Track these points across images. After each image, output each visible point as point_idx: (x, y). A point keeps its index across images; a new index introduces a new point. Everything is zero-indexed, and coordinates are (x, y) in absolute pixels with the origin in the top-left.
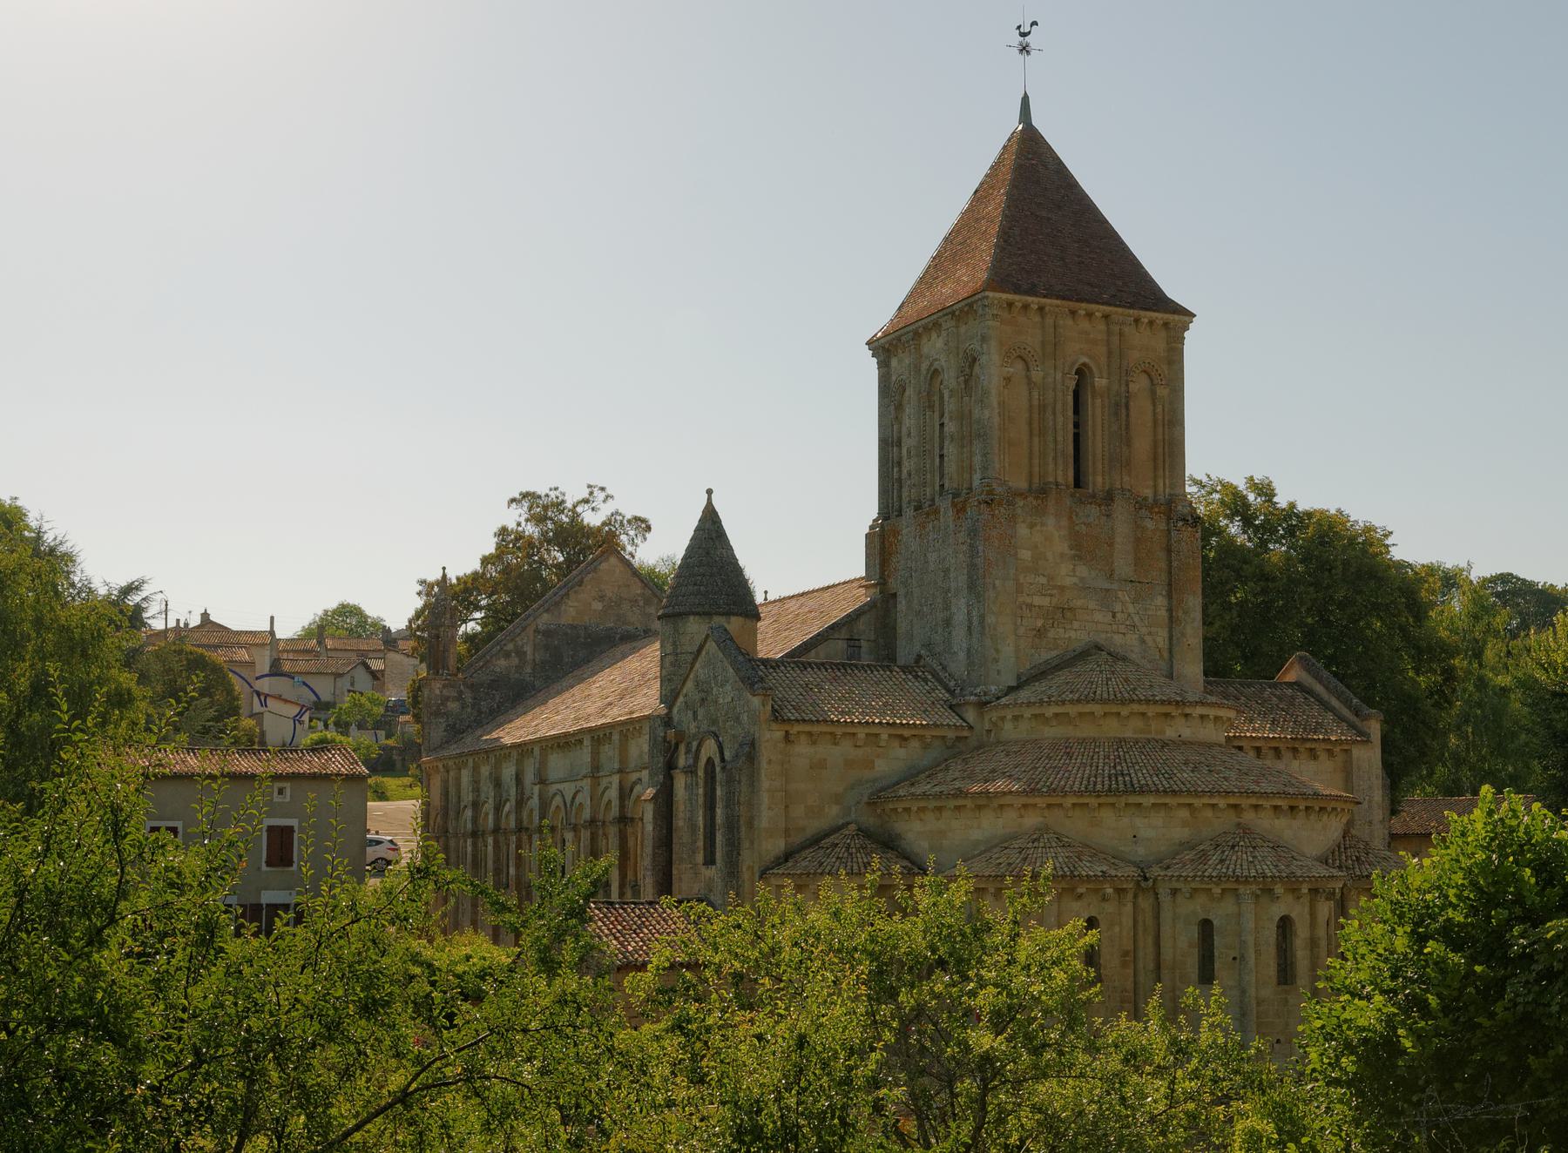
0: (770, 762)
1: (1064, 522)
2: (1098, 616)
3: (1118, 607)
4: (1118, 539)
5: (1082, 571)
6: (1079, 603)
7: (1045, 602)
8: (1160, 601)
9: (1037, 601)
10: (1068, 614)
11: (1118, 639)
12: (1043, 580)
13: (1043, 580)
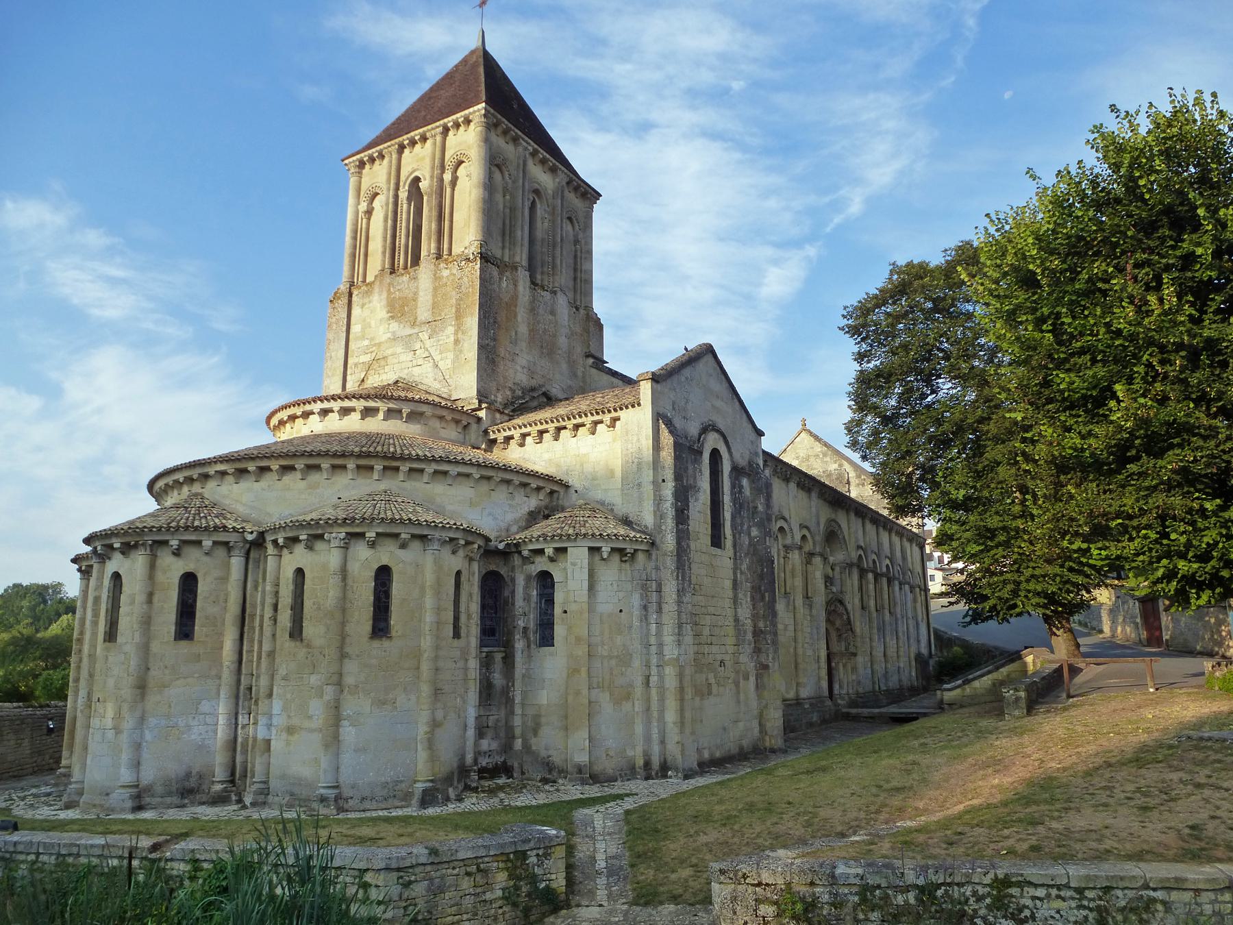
1: (385, 295)
2: (403, 358)
3: (417, 346)
4: (421, 294)
5: (394, 326)
6: (389, 352)
7: (366, 358)
10: (382, 363)
11: (416, 371)
13: (366, 343)
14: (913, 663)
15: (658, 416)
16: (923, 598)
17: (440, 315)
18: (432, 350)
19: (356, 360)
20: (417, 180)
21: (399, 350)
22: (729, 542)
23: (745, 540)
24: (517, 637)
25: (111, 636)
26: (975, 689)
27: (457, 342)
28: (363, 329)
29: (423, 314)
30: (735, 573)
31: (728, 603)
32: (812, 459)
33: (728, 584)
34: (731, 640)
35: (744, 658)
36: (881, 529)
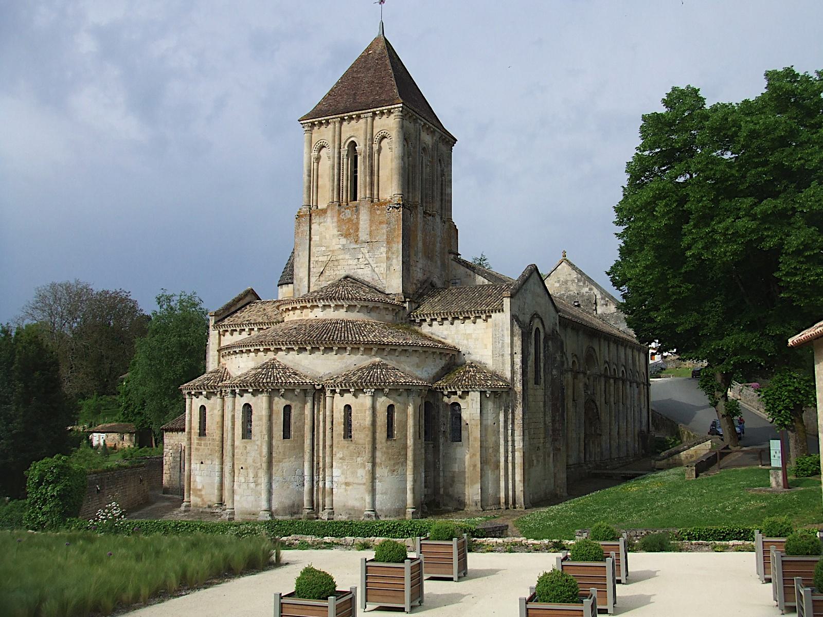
0: (213, 344)
2: (350, 262)
5: (343, 241)
6: (340, 257)
7: (325, 259)
8: (383, 250)
9: (321, 259)
10: (336, 263)
12: (324, 249)
13: (324, 249)
14: (637, 438)
15: (514, 317)
16: (646, 390)
17: (375, 238)
18: (370, 260)
19: (317, 259)
20: (353, 145)
21: (347, 257)
22: (542, 381)
23: (550, 377)
24: (441, 436)
25: (247, 433)
26: (675, 459)
27: (388, 258)
28: (321, 239)
29: (363, 235)
30: (545, 398)
31: (541, 415)
32: (569, 283)
33: (542, 404)
34: (542, 436)
35: (548, 445)
36: (620, 346)
